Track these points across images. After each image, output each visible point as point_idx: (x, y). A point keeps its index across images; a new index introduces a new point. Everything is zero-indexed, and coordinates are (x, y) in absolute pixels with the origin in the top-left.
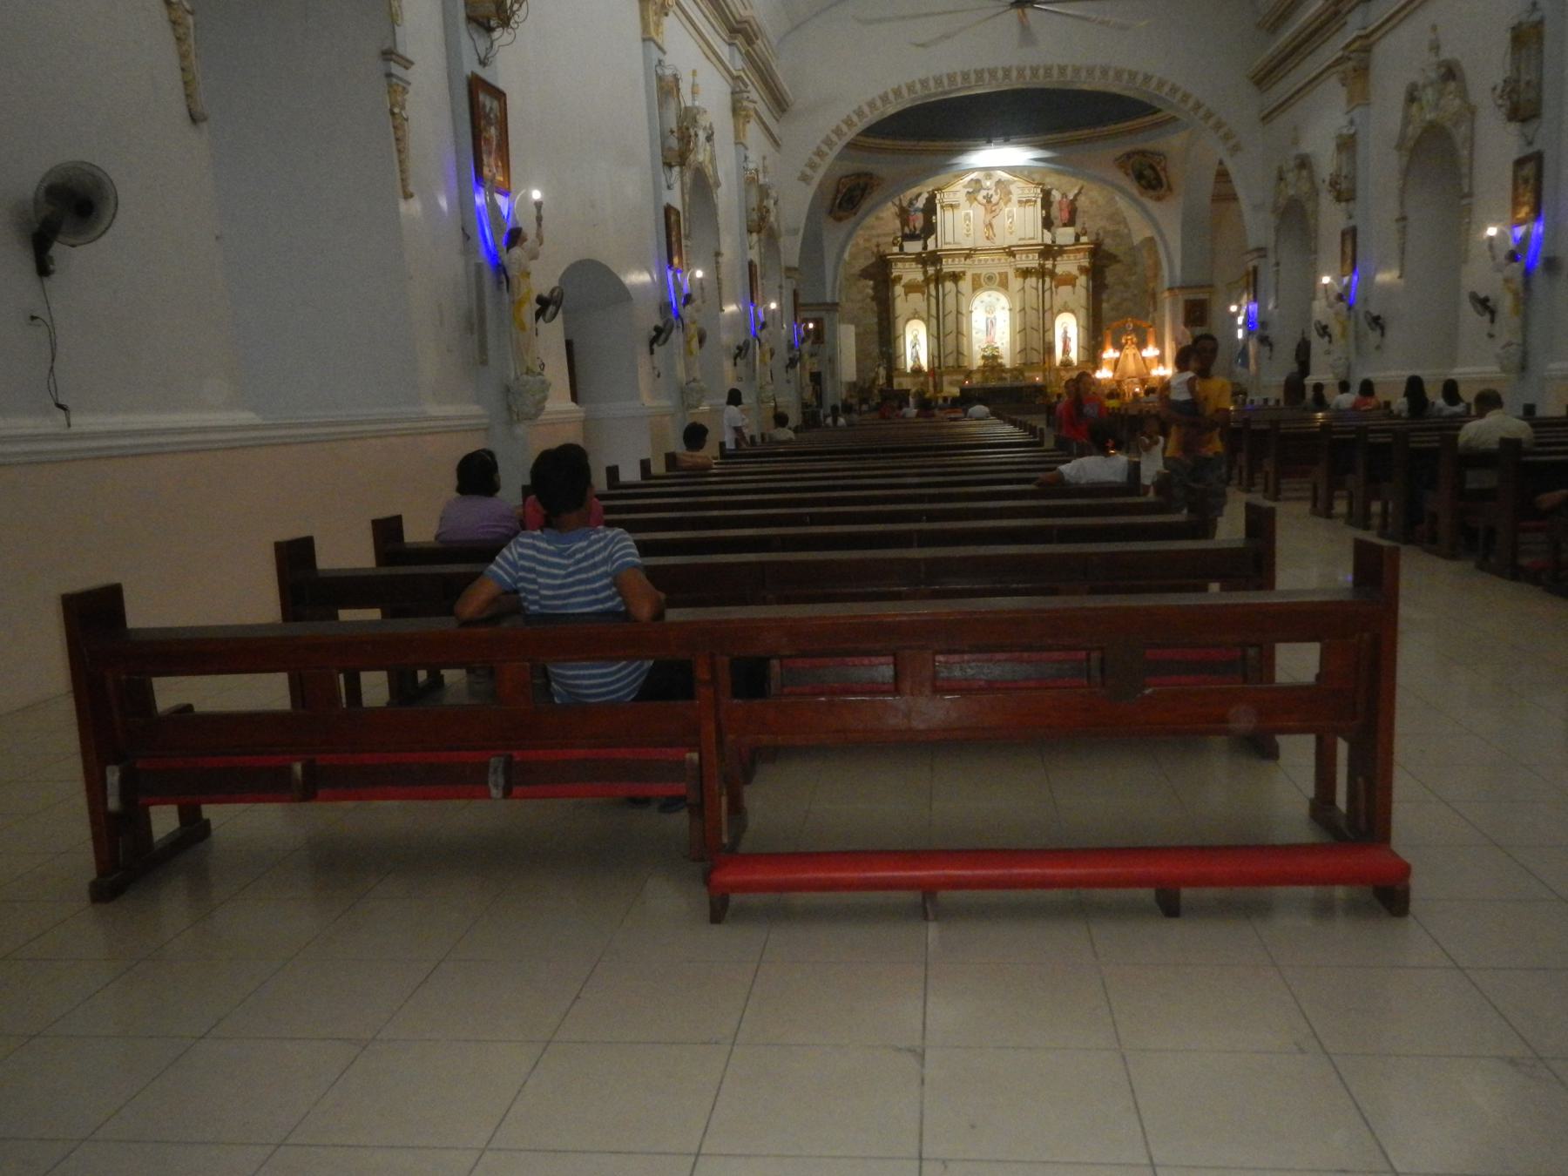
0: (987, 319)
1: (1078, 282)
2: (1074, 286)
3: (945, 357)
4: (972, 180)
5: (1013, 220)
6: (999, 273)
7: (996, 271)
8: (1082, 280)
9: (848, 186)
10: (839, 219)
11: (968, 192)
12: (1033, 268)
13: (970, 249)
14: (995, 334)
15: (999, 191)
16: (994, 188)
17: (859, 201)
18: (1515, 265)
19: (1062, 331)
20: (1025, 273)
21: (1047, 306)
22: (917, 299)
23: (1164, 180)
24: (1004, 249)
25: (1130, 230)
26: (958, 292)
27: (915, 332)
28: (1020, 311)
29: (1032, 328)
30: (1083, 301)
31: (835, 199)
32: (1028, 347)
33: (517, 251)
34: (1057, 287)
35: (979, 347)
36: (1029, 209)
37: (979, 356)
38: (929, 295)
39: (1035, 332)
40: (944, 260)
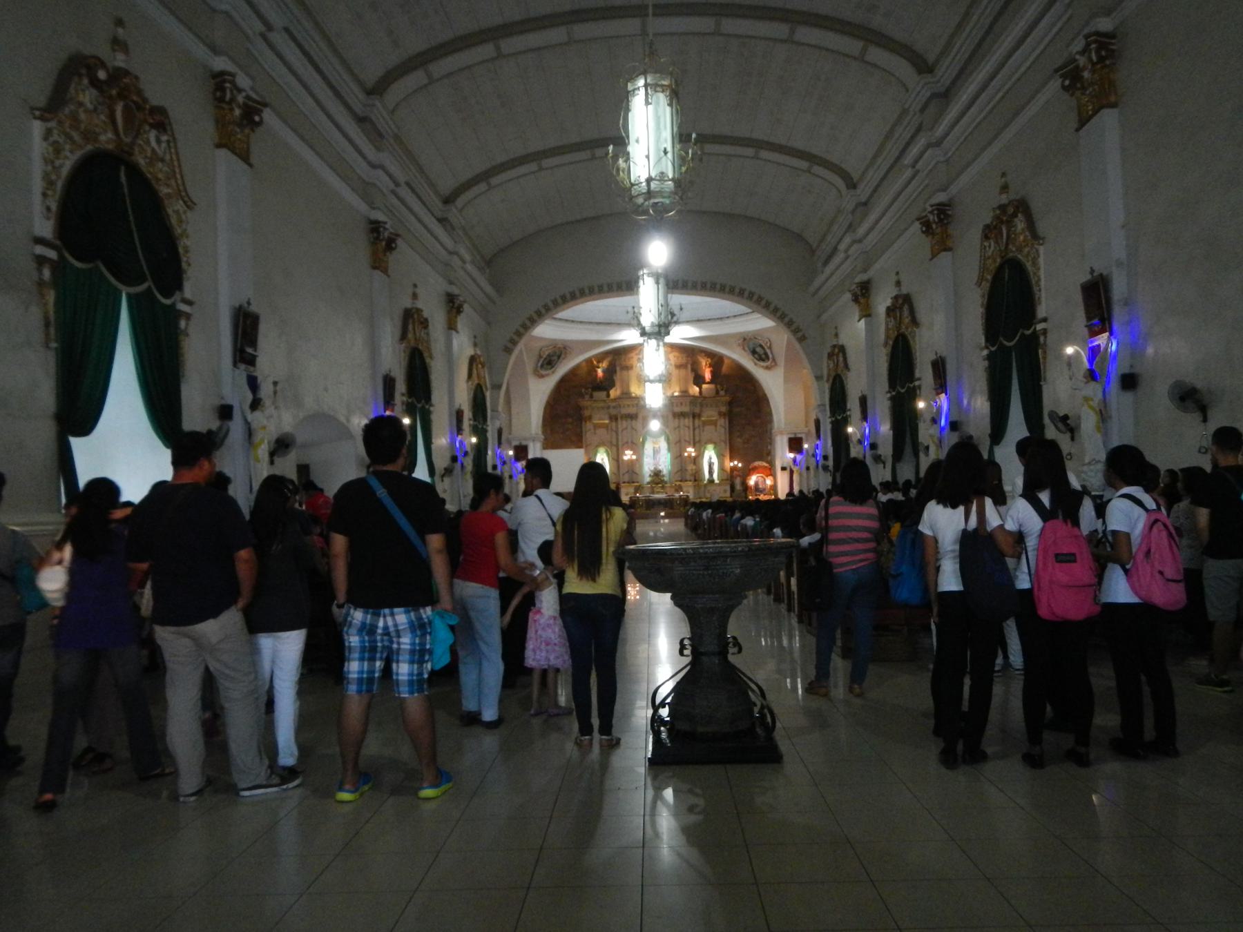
0: (654, 448)
1: (719, 423)
2: (716, 426)
3: (624, 474)
8: (723, 422)
9: (547, 353)
10: (542, 376)
14: (659, 458)
17: (555, 364)
18: (935, 426)
20: (682, 415)
21: (697, 439)
22: (601, 432)
23: (770, 356)
26: (633, 428)
27: (602, 457)
28: (676, 444)
30: (723, 438)
31: (539, 361)
33: (257, 414)
34: (703, 426)
35: (649, 468)
36: (683, 372)
37: (648, 475)
38: (612, 430)
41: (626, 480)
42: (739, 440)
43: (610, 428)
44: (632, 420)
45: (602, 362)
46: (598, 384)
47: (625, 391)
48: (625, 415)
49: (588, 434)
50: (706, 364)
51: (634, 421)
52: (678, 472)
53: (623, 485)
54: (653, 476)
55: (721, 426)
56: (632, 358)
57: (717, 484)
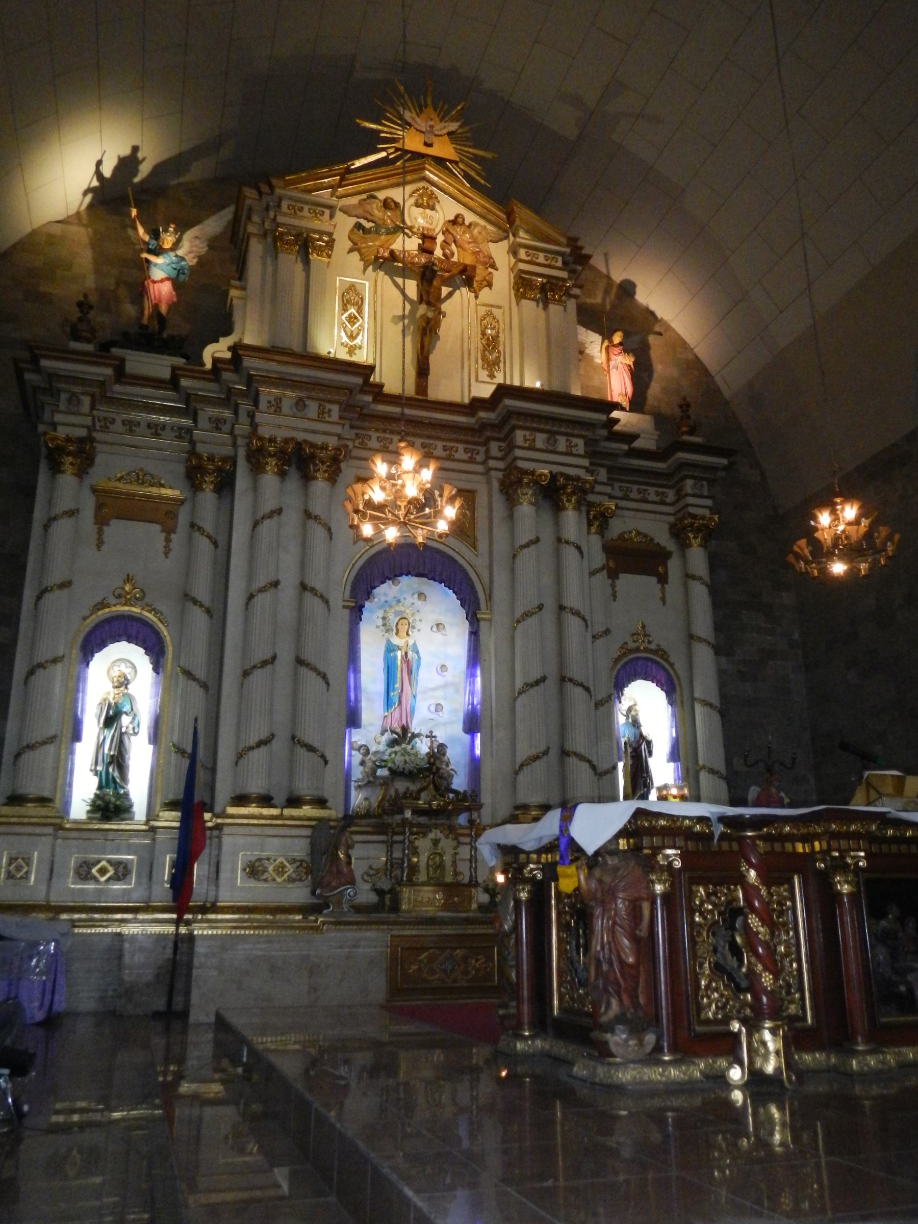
0: (390, 649)
1: (674, 566)
2: (663, 579)
4: (374, 197)
11: (358, 226)
12: (578, 479)
14: (415, 697)
16: (440, 238)
24: (477, 404)
25: (762, 474)
26: (308, 515)
27: (127, 671)
34: (613, 575)
39: (579, 690)
41: (255, 787)
43: (183, 518)
46: (142, 327)
48: (286, 441)
49: (63, 528)
52: (536, 758)
53: (231, 810)
54: (385, 783)
56: (332, 216)
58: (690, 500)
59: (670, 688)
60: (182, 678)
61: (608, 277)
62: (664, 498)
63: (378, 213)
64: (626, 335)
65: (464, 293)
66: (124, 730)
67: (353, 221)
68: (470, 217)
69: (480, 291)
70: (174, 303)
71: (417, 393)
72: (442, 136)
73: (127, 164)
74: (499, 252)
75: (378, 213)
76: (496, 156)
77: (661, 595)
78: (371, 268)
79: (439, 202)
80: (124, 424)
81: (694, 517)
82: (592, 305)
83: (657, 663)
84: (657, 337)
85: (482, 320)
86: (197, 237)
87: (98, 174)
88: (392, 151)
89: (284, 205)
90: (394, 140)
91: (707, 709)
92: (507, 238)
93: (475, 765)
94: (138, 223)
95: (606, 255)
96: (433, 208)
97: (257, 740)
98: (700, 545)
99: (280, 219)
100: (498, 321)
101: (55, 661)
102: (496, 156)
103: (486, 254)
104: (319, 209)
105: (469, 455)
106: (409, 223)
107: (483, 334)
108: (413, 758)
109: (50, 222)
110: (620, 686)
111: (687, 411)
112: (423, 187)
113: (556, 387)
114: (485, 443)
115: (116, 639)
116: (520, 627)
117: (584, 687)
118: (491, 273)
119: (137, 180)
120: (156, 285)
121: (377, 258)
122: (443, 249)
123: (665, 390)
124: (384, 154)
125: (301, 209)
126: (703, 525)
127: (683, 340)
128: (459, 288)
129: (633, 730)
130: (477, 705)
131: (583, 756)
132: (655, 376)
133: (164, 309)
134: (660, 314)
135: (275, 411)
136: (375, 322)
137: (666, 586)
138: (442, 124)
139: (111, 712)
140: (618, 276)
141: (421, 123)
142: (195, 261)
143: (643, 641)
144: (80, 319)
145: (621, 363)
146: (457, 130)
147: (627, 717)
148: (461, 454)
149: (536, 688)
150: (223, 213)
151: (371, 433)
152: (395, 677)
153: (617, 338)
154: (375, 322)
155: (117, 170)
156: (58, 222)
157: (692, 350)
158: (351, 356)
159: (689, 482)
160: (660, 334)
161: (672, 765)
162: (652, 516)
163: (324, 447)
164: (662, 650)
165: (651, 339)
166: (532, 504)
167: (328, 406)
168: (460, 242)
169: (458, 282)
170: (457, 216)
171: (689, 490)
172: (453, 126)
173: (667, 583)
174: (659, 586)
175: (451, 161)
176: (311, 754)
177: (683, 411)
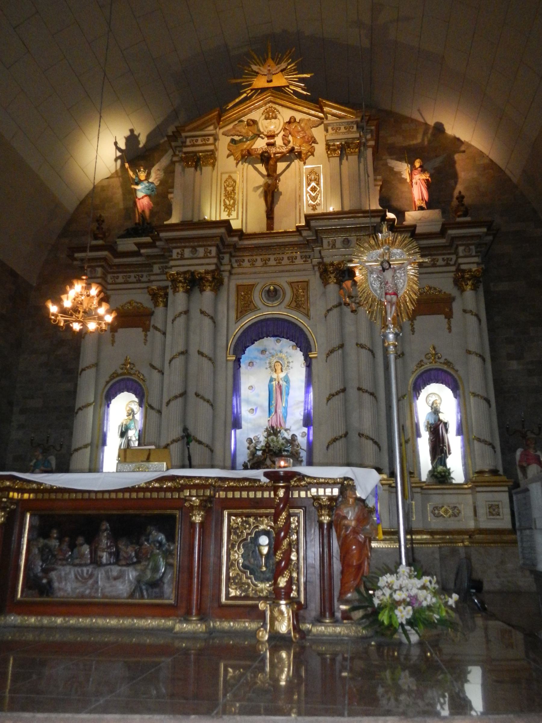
0: (271, 380)
1: (457, 307)
2: (449, 316)
4: (242, 121)
5: (318, 184)
6: (291, 284)
7: (283, 281)
11: (233, 141)
13: (226, 224)
14: (286, 408)
15: (290, 138)
16: (282, 133)
19: (429, 410)
24: (299, 229)
26: (202, 312)
29: (359, 389)
32: (353, 436)
40: (175, 252)
42: (514, 365)
44: (202, 291)
45: (148, 169)
46: (136, 224)
47: (188, 218)
48: (185, 273)
50: (413, 167)
51: (208, 294)
52: (335, 440)
55: (465, 311)
56: (216, 139)
57: (459, 486)
58: (460, 261)
59: (455, 388)
60: (149, 408)
61: (426, 124)
62: (449, 262)
63: (243, 129)
64: (423, 160)
65: (296, 163)
66: (129, 438)
67: (229, 139)
68: (298, 116)
69: (306, 159)
70: (152, 207)
71: (268, 229)
72: (277, 73)
73: (132, 139)
74: (318, 133)
75: (243, 129)
76: (313, 74)
77: (447, 326)
78: (240, 163)
79: (279, 113)
80: (123, 278)
81: (463, 271)
82: (414, 145)
83: (446, 372)
84: (461, 154)
85: (308, 177)
86: (159, 170)
87: (118, 148)
88: (249, 91)
89: (188, 140)
90: (250, 85)
91: (476, 398)
92: (322, 123)
93: (310, 444)
94: (129, 170)
95: (419, 110)
96: (275, 118)
97: (171, 440)
98: (471, 289)
99: (185, 150)
100: (318, 176)
101: (88, 405)
102: (313, 74)
103: (310, 136)
104: (207, 138)
105: (304, 259)
106: (262, 130)
107: (309, 185)
108: (276, 444)
109: (102, 180)
110: (417, 388)
111: (462, 201)
112: (269, 107)
113: (355, 207)
114: (313, 250)
115: (122, 391)
116: (329, 358)
117: (369, 393)
118: (313, 147)
119: (141, 146)
120: (140, 200)
121: (243, 156)
122: (283, 139)
123: (467, 189)
124: (245, 95)
125: (197, 141)
126: (471, 275)
127: (481, 151)
128: (294, 161)
129: (434, 416)
130: (311, 409)
131: (368, 436)
132: (460, 180)
133: (147, 212)
134: (463, 139)
135: (181, 257)
136: (243, 193)
137: (451, 319)
138: (277, 67)
139: (123, 430)
140: (431, 122)
141: (264, 70)
142: (159, 182)
143: (435, 358)
144: (98, 228)
145: (419, 179)
146: (287, 67)
147: (432, 408)
148: (299, 261)
149: (337, 397)
150: (167, 154)
151: (245, 258)
152: (272, 396)
153: (417, 164)
154: (243, 193)
155: (127, 144)
156: (108, 178)
157: (488, 156)
158: (229, 216)
159: (461, 249)
160: (464, 152)
161: (459, 438)
162: (441, 275)
163: (207, 272)
164: (449, 362)
165: (457, 157)
166: (336, 283)
167: (209, 248)
168: (292, 133)
169: (292, 157)
170: (290, 119)
171: (461, 254)
172: (283, 65)
173: (452, 318)
174: (447, 320)
175: (284, 87)
176: (201, 446)
177: (459, 202)
